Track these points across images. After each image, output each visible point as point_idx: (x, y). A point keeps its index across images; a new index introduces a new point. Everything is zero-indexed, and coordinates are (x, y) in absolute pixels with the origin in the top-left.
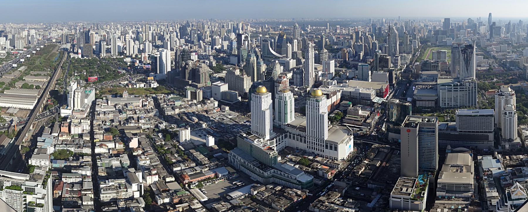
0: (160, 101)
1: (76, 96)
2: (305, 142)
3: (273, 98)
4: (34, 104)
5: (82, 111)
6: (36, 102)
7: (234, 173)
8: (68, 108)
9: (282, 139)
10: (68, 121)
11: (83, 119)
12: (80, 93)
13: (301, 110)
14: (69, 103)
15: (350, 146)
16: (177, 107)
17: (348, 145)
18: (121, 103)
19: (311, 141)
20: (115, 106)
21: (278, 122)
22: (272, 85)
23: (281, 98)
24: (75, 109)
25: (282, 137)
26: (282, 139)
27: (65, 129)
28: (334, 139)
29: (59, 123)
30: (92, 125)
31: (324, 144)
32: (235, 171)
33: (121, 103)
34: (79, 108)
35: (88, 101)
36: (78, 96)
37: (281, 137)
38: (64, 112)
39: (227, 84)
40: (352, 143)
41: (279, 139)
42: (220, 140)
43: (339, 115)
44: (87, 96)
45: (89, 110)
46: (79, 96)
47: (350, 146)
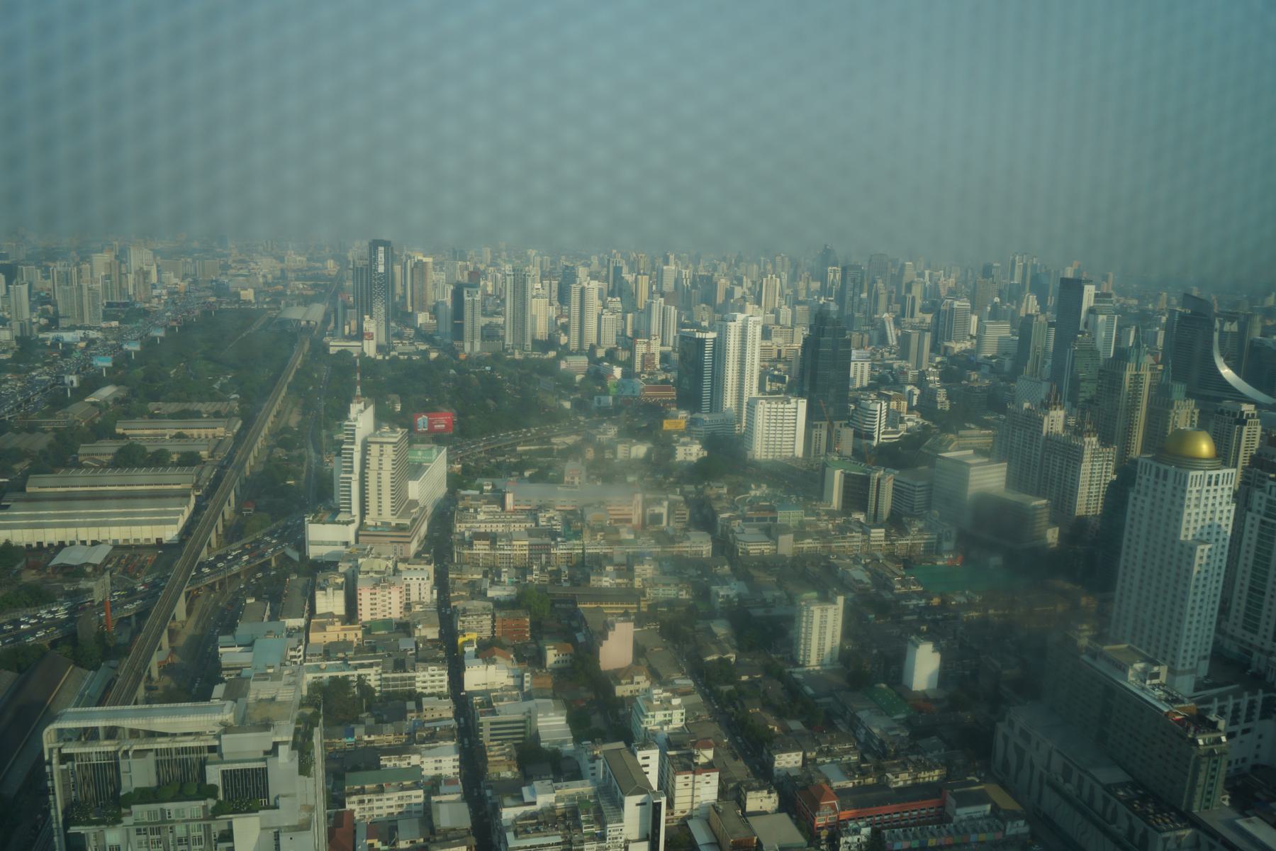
0: (717, 506)
1: (373, 462)
4: (182, 520)
5: (399, 528)
6: (187, 511)
8: (341, 517)
9: (1249, 719)
10: (343, 567)
11: (405, 560)
12: (389, 449)
14: (339, 498)
16: (784, 529)
18: (561, 500)
20: (533, 514)
24: (369, 521)
25: (1252, 705)
26: (1249, 719)
27: (330, 602)
29: (303, 580)
30: (441, 582)
33: (561, 500)
34: (388, 516)
35: (427, 488)
36: (384, 464)
38: (324, 537)
44: (416, 470)
45: (424, 529)
46: (388, 465)
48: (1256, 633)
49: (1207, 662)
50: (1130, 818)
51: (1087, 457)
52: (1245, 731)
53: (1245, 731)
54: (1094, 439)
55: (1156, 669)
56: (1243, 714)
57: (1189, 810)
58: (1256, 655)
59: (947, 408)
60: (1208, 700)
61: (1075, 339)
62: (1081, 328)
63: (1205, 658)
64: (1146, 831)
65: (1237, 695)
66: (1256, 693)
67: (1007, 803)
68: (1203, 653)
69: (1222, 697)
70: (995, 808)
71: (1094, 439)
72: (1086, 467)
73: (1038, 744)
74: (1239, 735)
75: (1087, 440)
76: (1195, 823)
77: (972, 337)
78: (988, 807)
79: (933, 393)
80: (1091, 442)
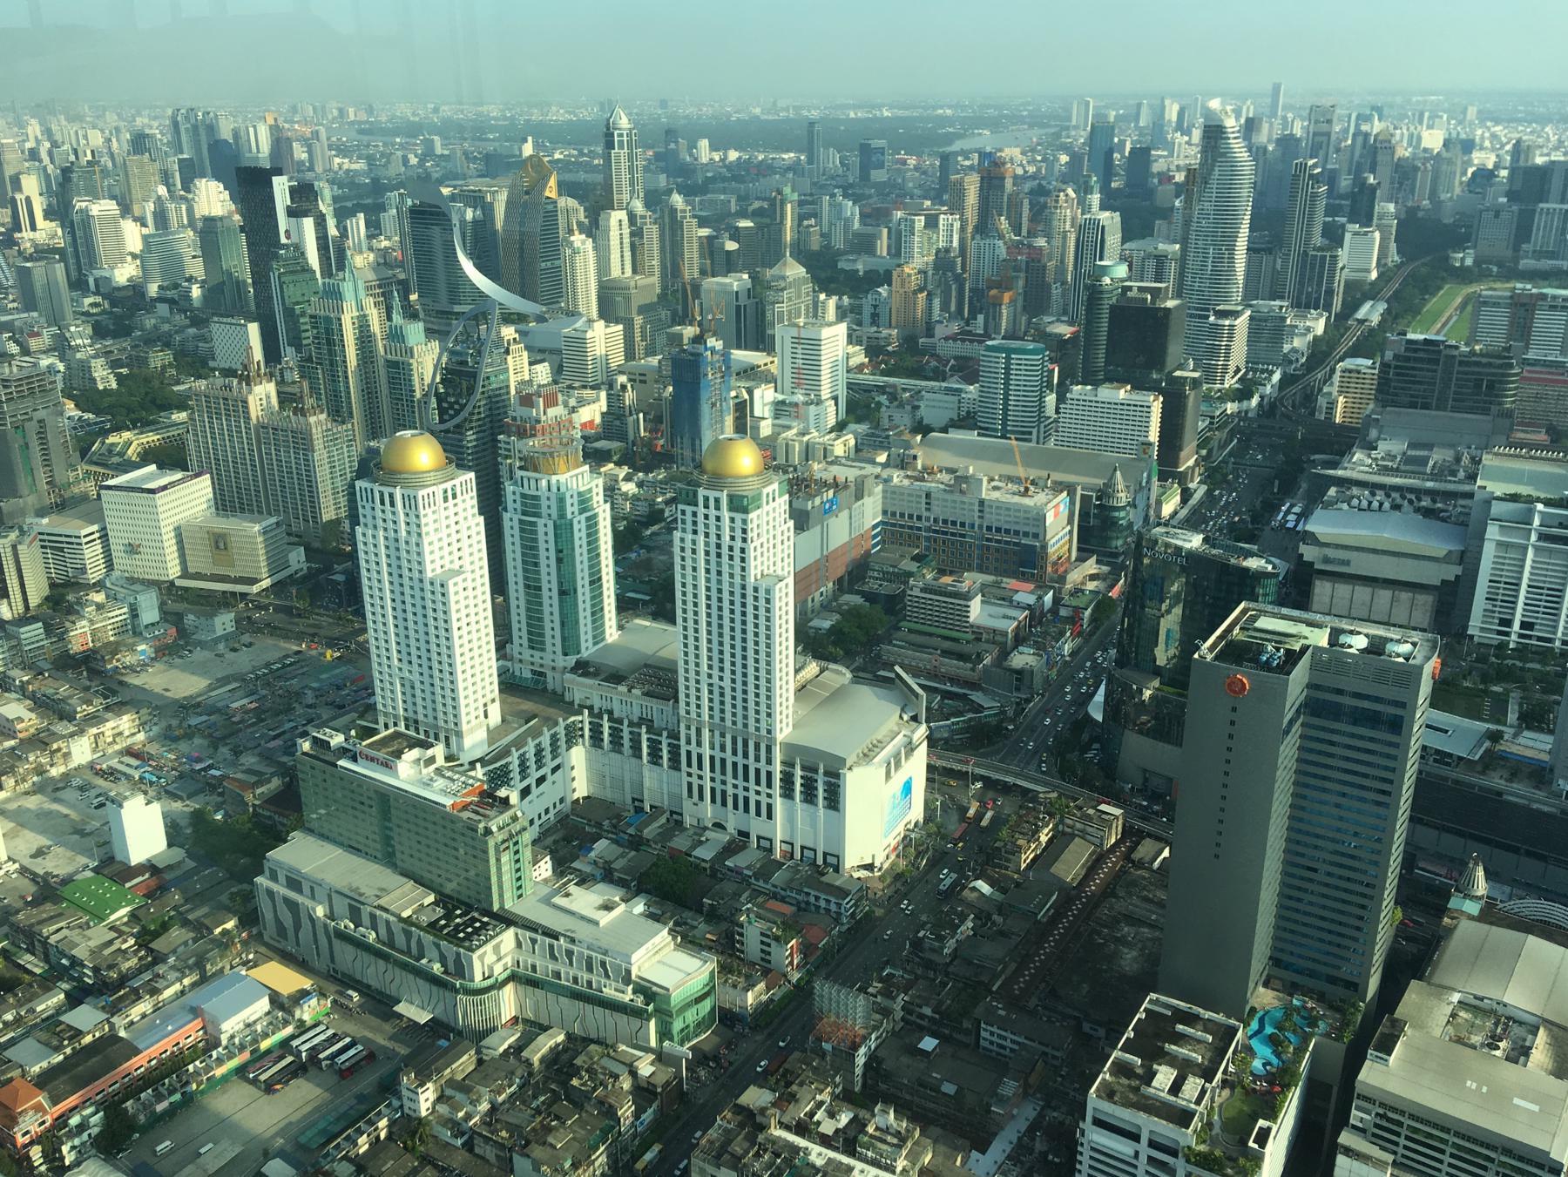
2: (675, 763)
3: (491, 504)
7: (304, 994)
13: (650, 592)
15: (908, 788)
17: (899, 778)
19: (707, 752)
21: (527, 654)
22: (484, 437)
23: (531, 505)
25: (554, 740)
28: (824, 736)
31: (777, 768)
32: (307, 983)
37: (545, 740)
39: (206, 481)
40: (917, 767)
41: (539, 753)
42: (198, 817)
43: (859, 626)
47: (908, 788)
48: (543, 650)
49: (498, 703)
50: (438, 946)
51: (318, 443)
52: (554, 770)
53: (554, 770)
54: (323, 417)
55: (430, 752)
56: (547, 753)
57: (502, 908)
58: (550, 674)
59: (114, 386)
60: (505, 752)
61: (276, 256)
62: (284, 240)
63: (493, 701)
64: (458, 954)
65: (536, 733)
66: (556, 724)
67: (287, 980)
68: (489, 697)
69: (519, 743)
70: (276, 1000)
71: (323, 417)
72: (320, 455)
73: (312, 889)
74: (550, 778)
75: (312, 419)
76: (507, 920)
77: (134, 256)
78: (263, 1004)
79: (85, 368)
80: (318, 422)
